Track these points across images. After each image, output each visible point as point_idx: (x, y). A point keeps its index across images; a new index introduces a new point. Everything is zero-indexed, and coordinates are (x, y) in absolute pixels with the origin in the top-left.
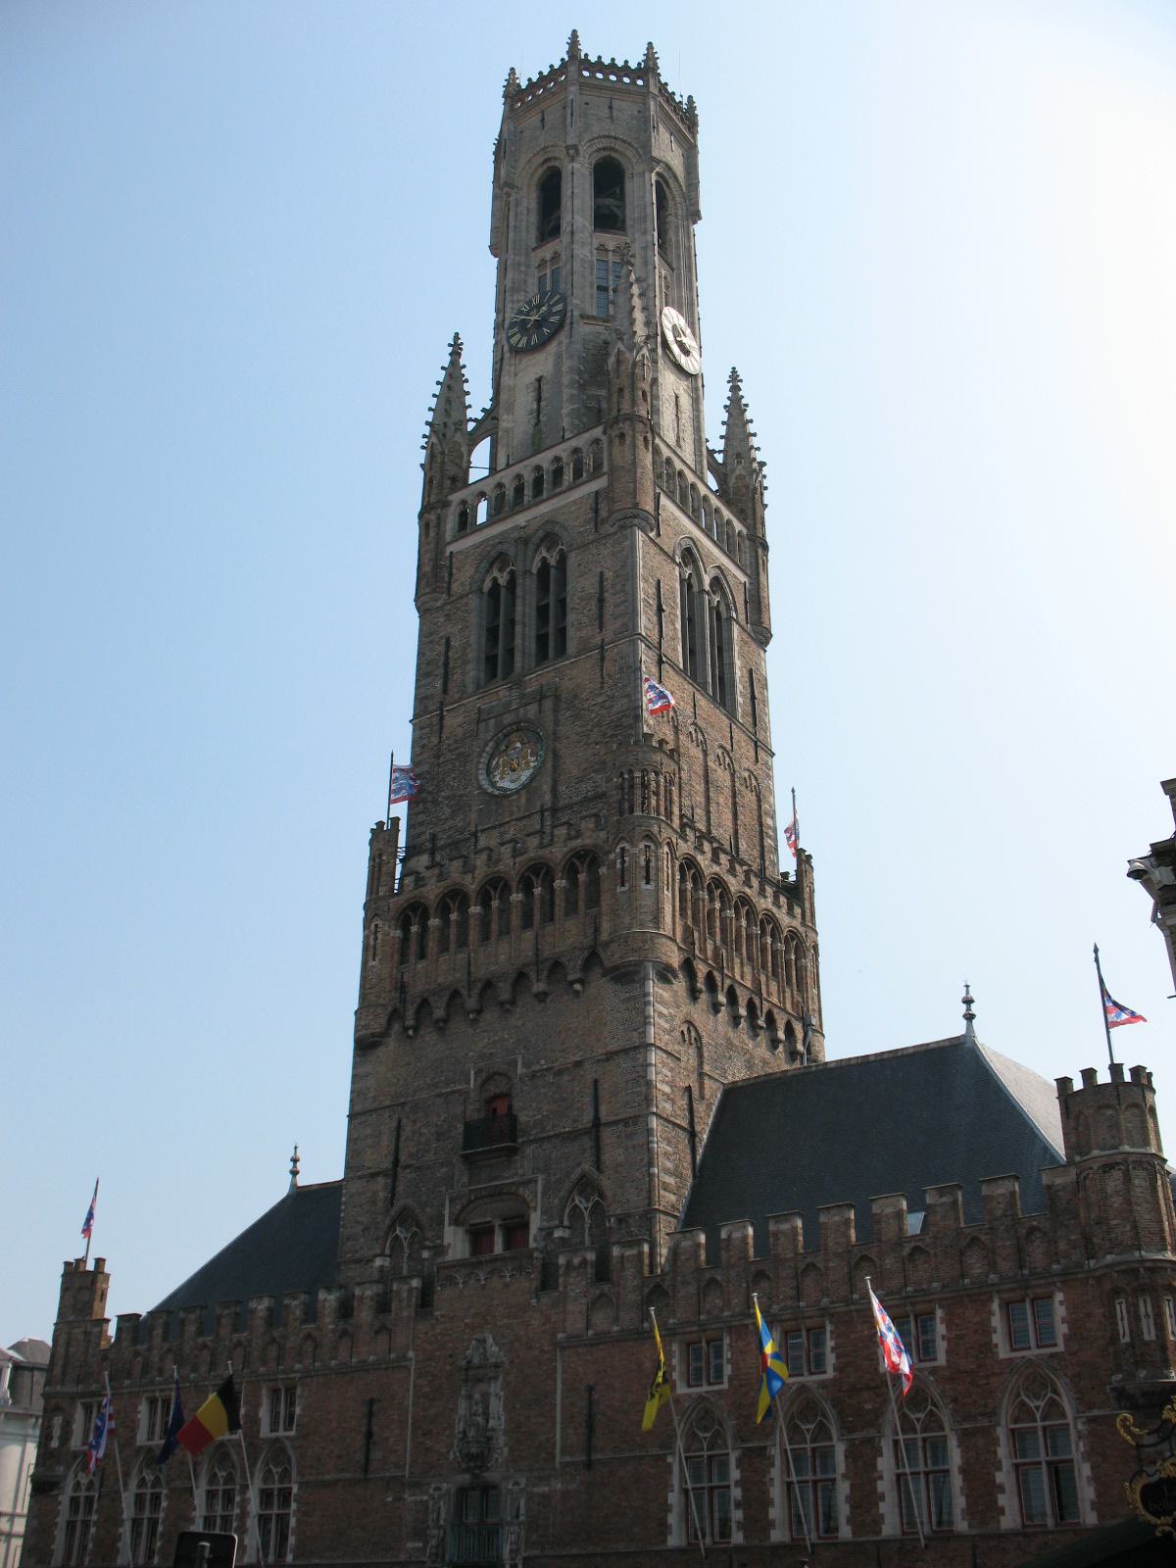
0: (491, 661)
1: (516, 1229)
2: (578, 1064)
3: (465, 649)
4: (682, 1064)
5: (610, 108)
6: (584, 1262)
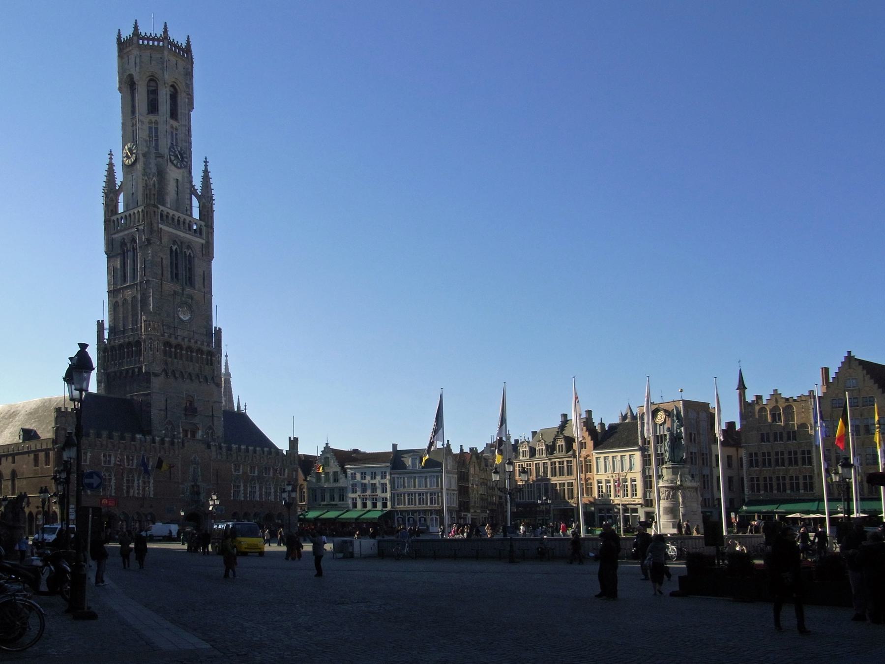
1: (194, 434)
2: (208, 401)
6: (215, 445)
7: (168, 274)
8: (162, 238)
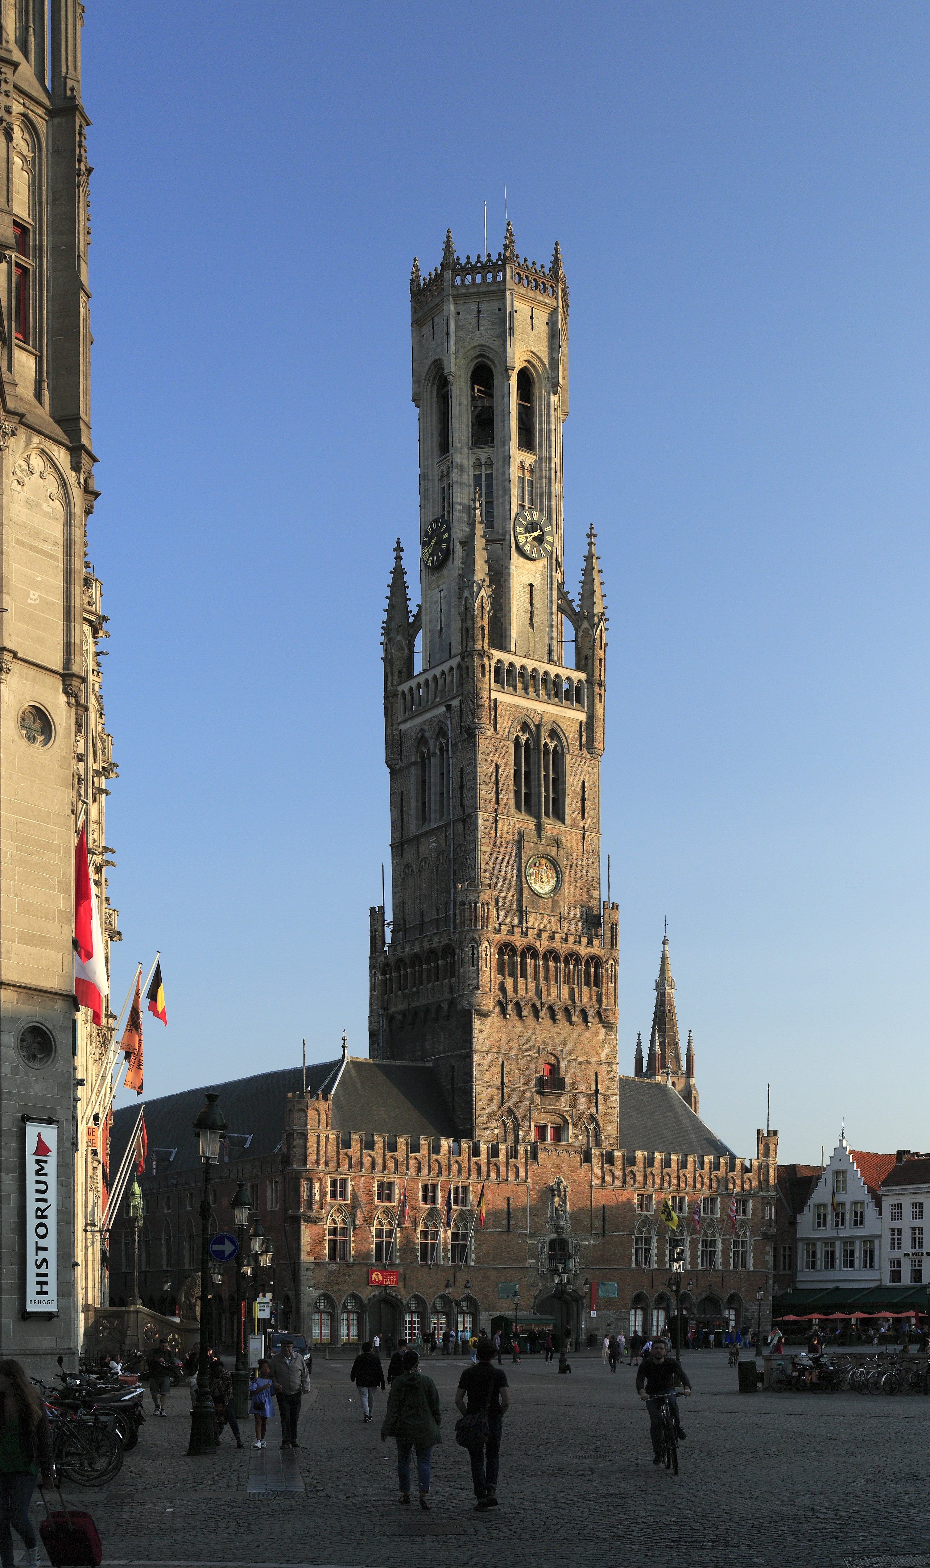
2: (588, 1062)
7: (508, 798)
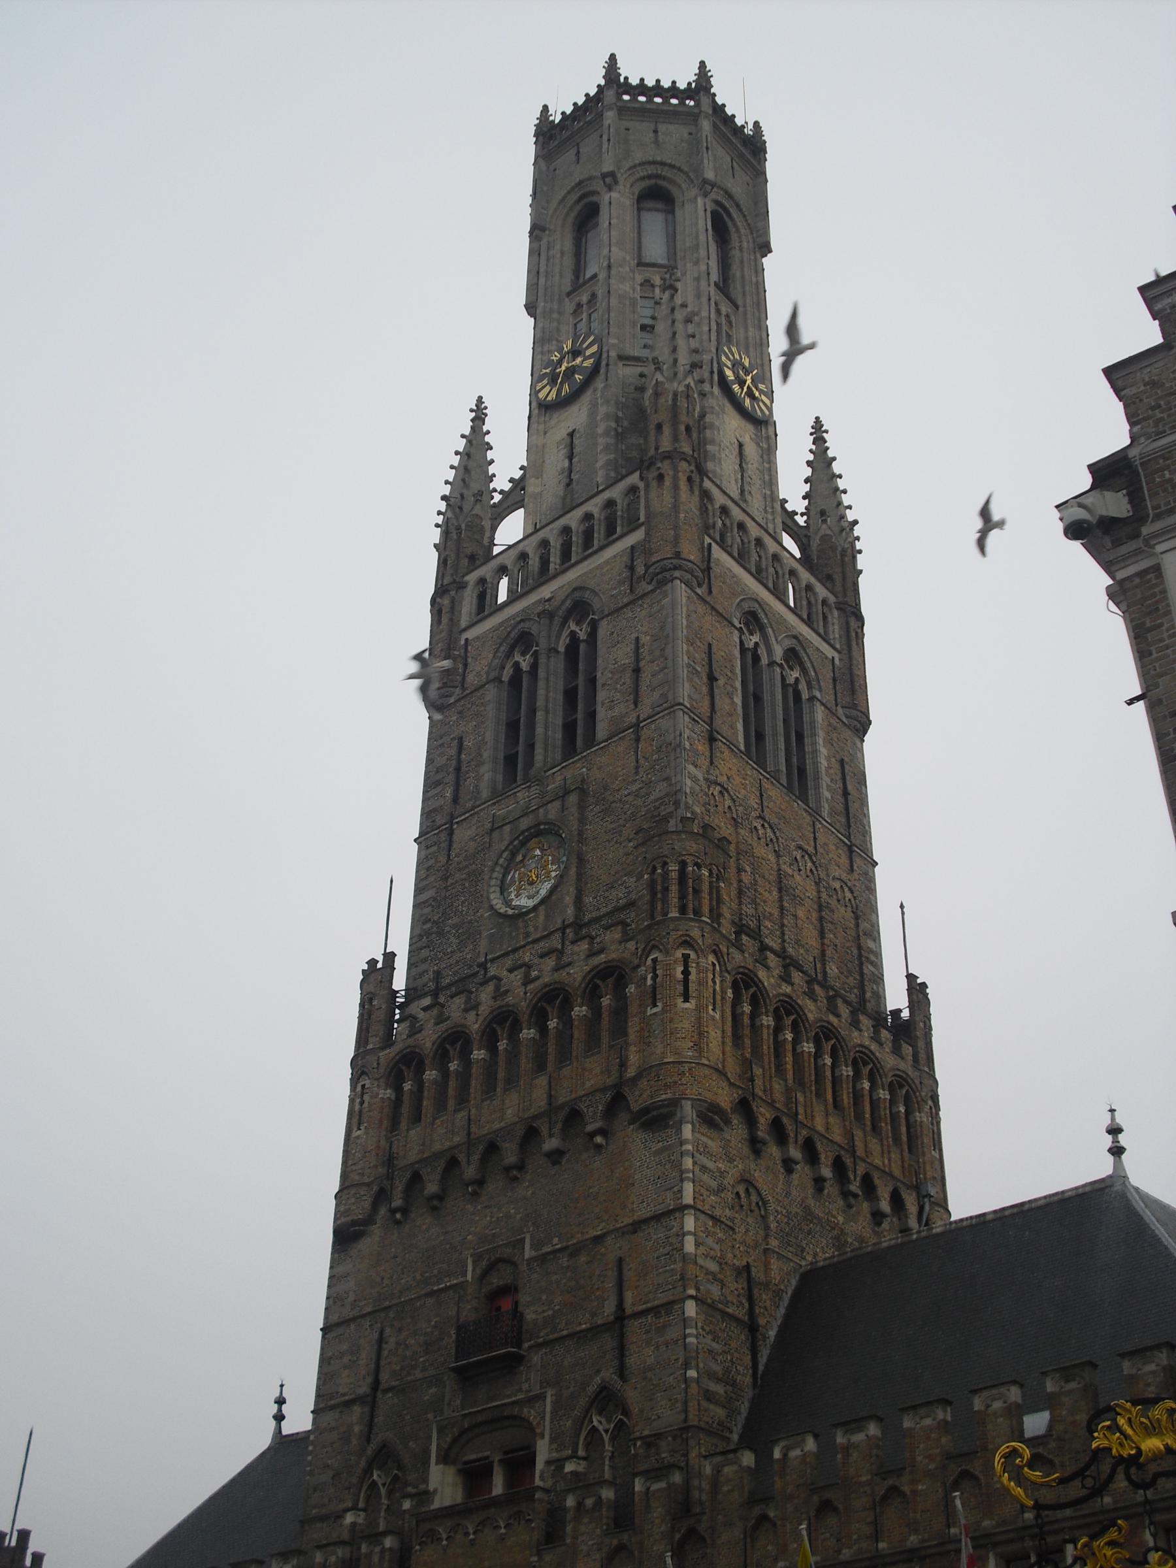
0: (511, 761)
2: (598, 1239)
3: (479, 748)
4: (738, 1237)
5: (656, 132)
8: (470, 668)
